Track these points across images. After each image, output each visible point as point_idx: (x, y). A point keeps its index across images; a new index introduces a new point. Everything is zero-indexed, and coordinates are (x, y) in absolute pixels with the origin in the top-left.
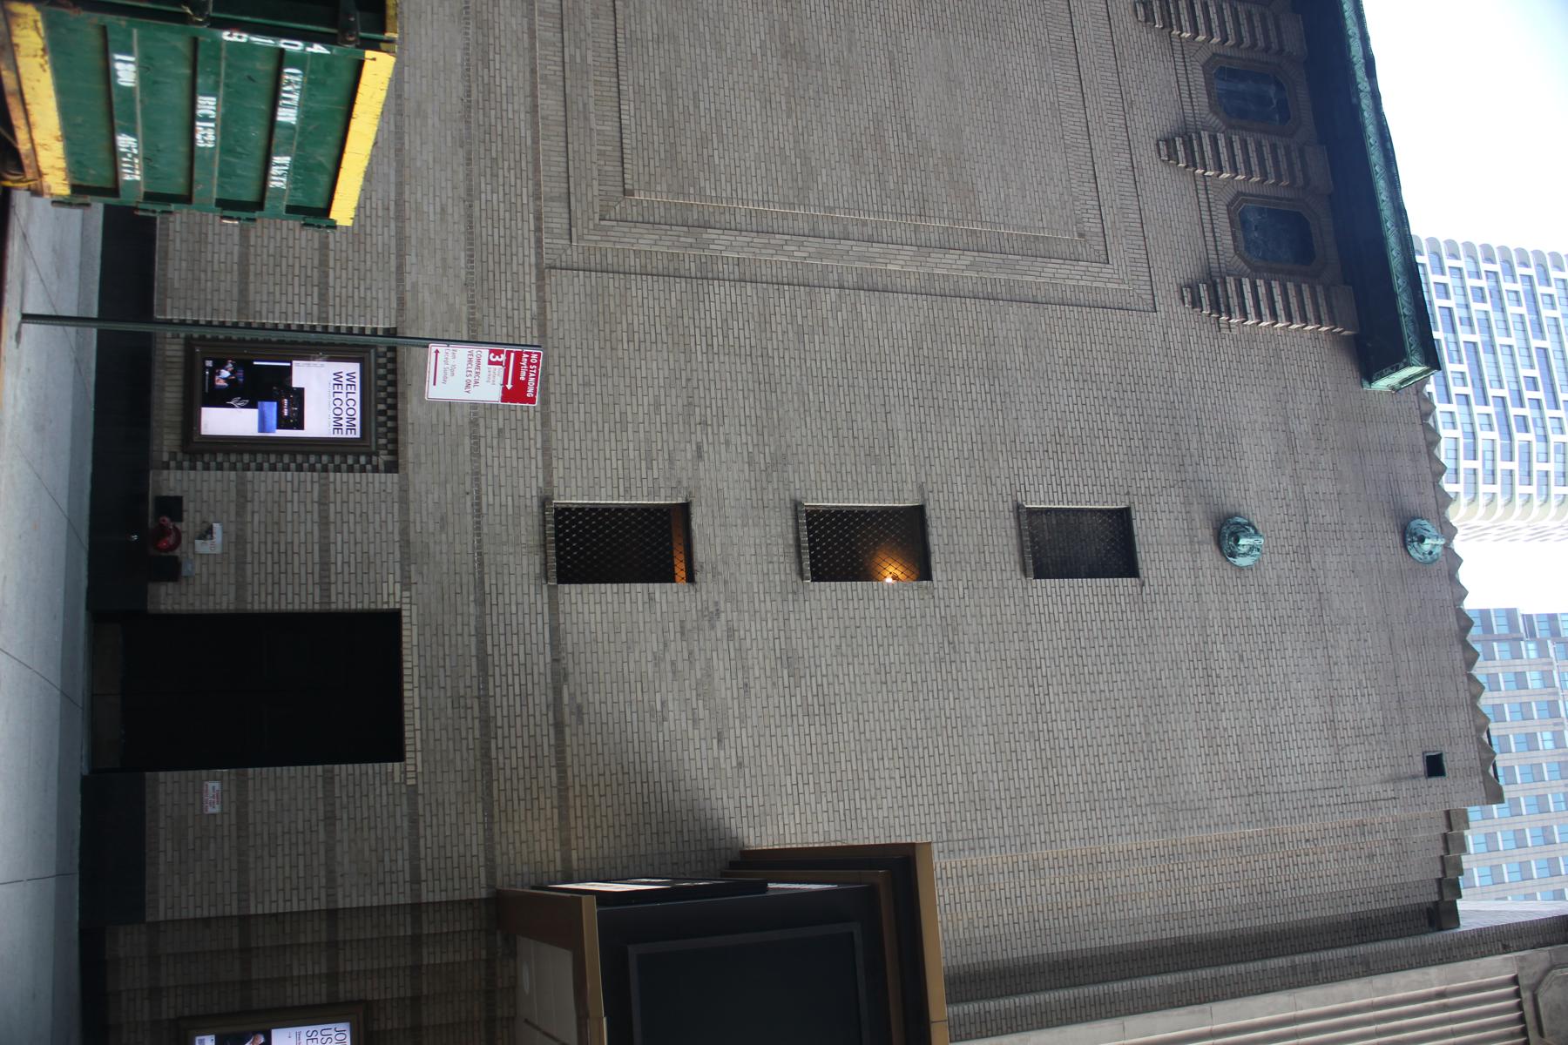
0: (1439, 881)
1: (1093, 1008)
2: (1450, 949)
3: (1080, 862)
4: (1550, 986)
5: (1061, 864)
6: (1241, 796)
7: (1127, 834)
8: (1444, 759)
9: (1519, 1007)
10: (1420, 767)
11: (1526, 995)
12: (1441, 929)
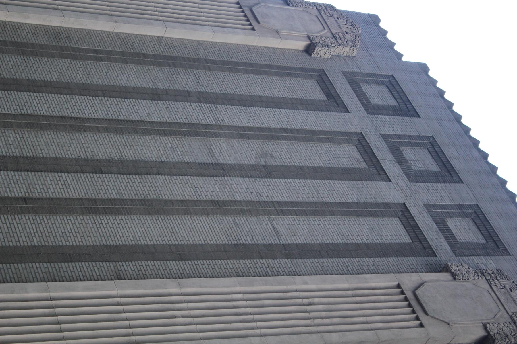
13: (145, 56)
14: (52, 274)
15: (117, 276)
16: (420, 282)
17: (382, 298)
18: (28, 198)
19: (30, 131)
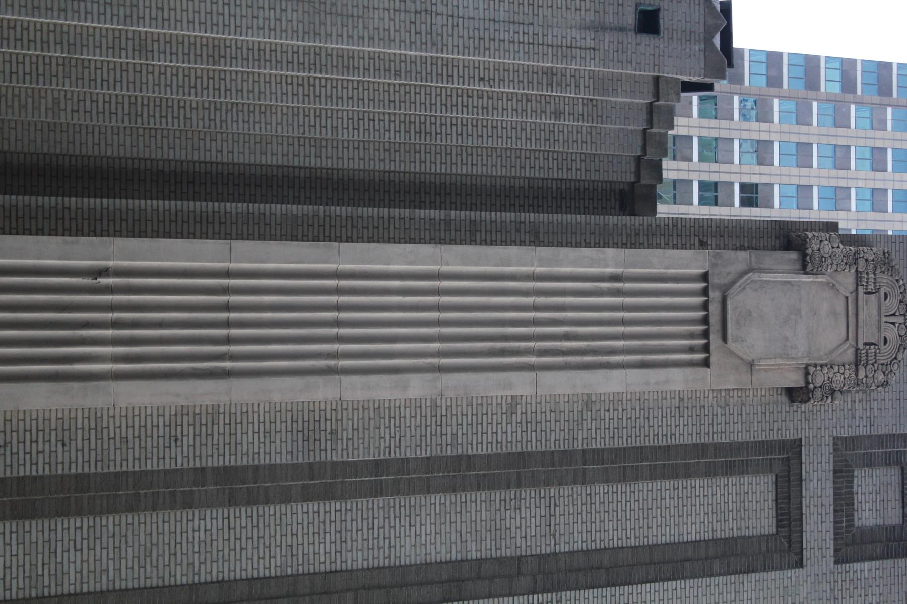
0: (638, 159)
1: (198, 226)
2: (637, 234)
3: (198, 52)
4: (744, 289)
5: (174, 50)
6: (405, 11)
7: (259, 28)
8: (661, 15)
9: (705, 306)
10: (630, 19)
11: (715, 295)
12: (633, 214)
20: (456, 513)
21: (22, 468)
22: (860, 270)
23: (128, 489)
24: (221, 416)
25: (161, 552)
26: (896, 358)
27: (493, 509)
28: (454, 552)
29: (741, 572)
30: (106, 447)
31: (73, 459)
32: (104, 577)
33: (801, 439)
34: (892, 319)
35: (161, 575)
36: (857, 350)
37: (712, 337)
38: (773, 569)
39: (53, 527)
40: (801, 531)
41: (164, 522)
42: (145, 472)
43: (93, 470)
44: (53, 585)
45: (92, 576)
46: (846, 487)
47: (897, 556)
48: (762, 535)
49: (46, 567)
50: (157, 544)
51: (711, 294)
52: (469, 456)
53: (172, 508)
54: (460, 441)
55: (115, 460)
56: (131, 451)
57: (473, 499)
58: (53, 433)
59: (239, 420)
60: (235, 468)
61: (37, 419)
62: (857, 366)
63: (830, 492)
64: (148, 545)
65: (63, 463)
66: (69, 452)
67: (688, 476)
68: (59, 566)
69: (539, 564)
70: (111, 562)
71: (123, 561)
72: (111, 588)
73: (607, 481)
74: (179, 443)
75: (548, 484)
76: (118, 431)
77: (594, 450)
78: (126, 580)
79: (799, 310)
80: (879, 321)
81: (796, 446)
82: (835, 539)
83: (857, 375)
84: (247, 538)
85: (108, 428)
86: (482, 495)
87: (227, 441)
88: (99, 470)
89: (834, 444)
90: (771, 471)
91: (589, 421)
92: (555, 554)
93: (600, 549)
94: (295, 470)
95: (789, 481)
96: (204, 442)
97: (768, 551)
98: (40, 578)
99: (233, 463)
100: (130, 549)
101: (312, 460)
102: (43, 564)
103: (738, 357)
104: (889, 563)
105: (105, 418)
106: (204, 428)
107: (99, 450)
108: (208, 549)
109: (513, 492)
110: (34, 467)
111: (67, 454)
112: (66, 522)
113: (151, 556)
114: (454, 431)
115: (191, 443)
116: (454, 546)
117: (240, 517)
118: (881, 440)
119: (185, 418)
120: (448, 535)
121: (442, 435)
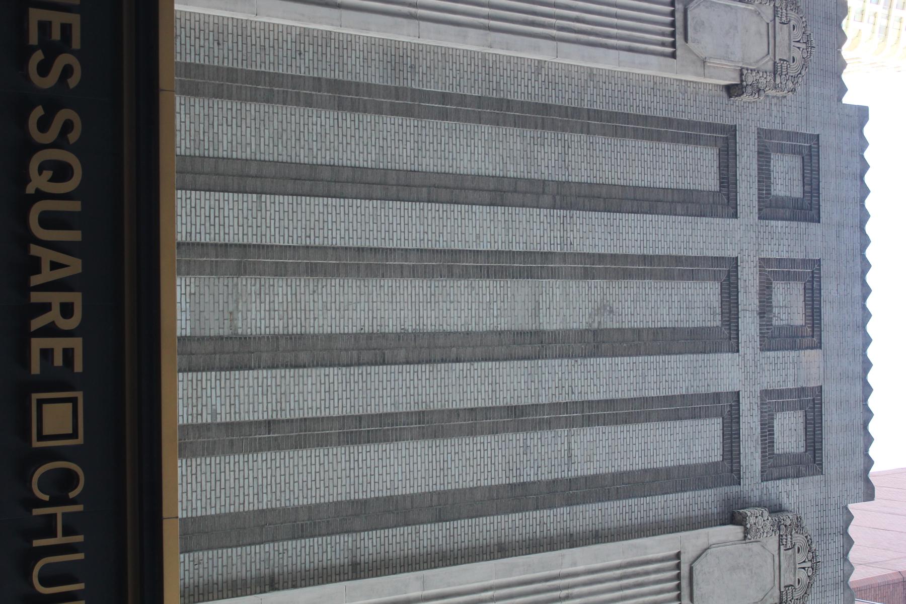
4: (699, 5)
9: (672, 14)
13: (509, 104)
14: (271, 562)
15: (352, 557)
16: (705, 547)
17: (653, 577)
18: (274, 421)
19: (309, 279)
20: (499, 141)
21: (188, 56)
22: (776, 5)
23: (265, 85)
24: (333, 41)
25: (289, 137)
26: (800, 73)
27: (525, 143)
28: (498, 170)
29: (695, 216)
30: (249, 50)
31: (226, 56)
32: (248, 149)
33: (736, 126)
34: (798, 45)
35: (289, 154)
36: (775, 63)
37: (677, 36)
38: (717, 216)
39: (211, 105)
40: (736, 192)
41: (291, 115)
42: (278, 74)
43: (240, 67)
44: (211, 149)
45: (239, 146)
46: (766, 165)
47: (799, 220)
48: (709, 191)
49: (206, 134)
50: (286, 130)
51: (676, 5)
52: (508, 101)
53: (297, 105)
54: (502, 88)
55: (256, 61)
56: (267, 57)
57: (511, 133)
58: (211, 34)
59: (345, 47)
60: (342, 83)
61: (199, 21)
62: (775, 74)
63: (755, 166)
64: (280, 130)
65: (218, 57)
66: (223, 49)
67: (659, 140)
68: (216, 136)
69: (558, 188)
70: (253, 138)
71: (262, 139)
72: (253, 158)
73: (604, 135)
74: (302, 57)
75: (563, 130)
76: (258, 40)
77: (595, 110)
78: (264, 154)
79: (736, 28)
80: (790, 44)
81: (733, 130)
82: (759, 202)
83: (775, 81)
84: (351, 136)
85: (251, 36)
86: (518, 131)
87: (337, 61)
88: (245, 67)
89: (758, 133)
90: (716, 146)
91: (592, 88)
92: (568, 182)
93: (600, 184)
94: (387, 91)
95: (728, 154)
96: (320, 58)
97: (714, 203)
98: (202, 142)
99: (341, 78)
100: (267, 131)
101: (397, 85)
102: (204, 132)
103: (695, 55)
104: (794, 224)
105: (249, 28)
106: (320, 48)
107: (244, 52)
108: (323, 140)
109: (539, 133)
110: (197, 57)
111: (221, 51)
112: (220, 103)
113: (282, 138)
114: (498, 80)
115: (311, 57)
116: (497, 165)
117: (346, 120)
118: (791, 135)
119: (307, 38)
120: (494, 157)
121: (489, 81)
